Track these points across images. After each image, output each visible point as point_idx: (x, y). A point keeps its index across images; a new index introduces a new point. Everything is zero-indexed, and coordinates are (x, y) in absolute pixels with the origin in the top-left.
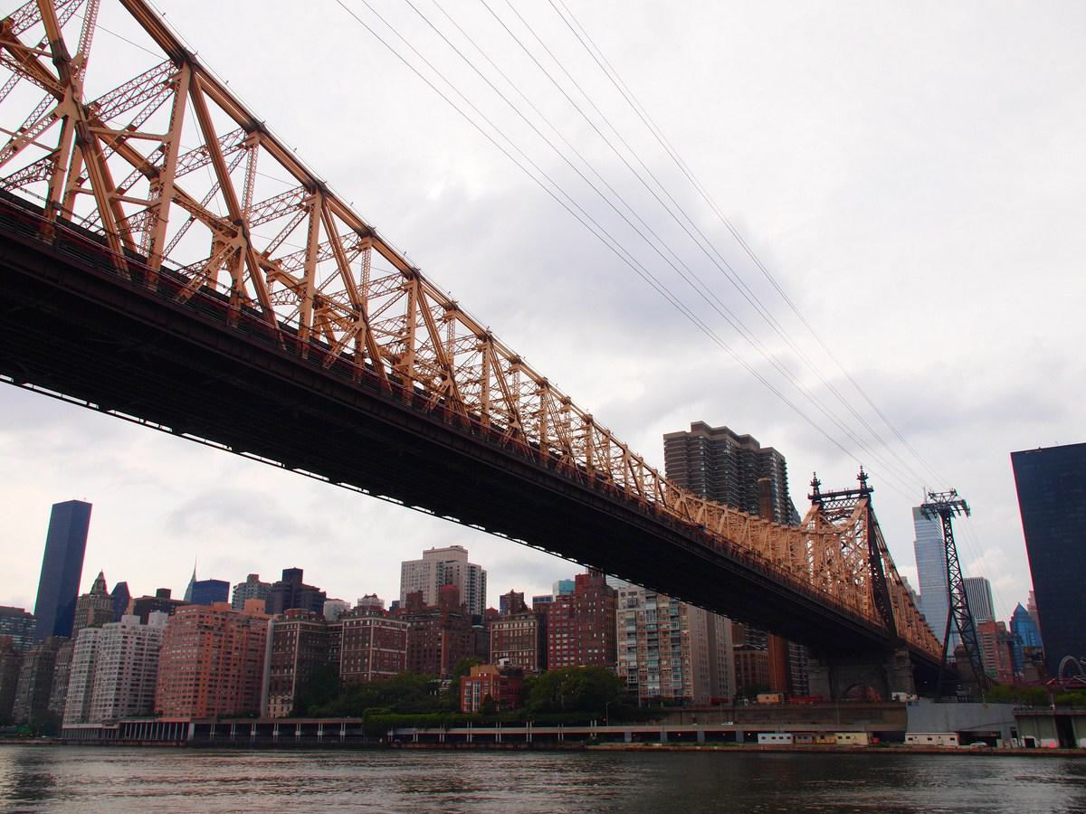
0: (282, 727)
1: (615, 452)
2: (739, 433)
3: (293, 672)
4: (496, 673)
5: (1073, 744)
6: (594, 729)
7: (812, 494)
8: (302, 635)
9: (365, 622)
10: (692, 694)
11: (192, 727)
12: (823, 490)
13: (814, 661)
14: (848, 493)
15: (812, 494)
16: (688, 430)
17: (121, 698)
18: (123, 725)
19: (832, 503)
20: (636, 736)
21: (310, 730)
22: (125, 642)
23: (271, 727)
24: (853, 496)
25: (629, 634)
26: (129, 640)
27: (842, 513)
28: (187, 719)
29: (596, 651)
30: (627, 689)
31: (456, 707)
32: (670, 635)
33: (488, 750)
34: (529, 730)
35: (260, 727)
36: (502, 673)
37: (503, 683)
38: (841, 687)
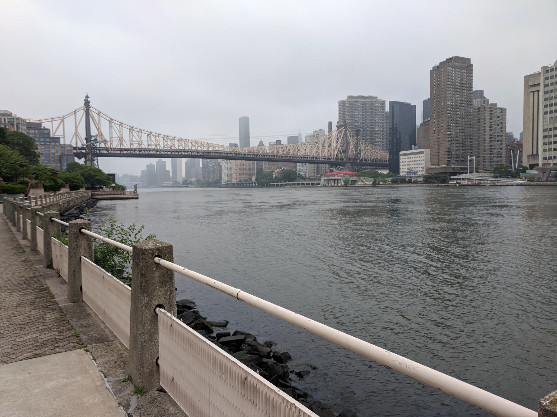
3: (255, 171)
4: (279, 171)
34: (279, 183)
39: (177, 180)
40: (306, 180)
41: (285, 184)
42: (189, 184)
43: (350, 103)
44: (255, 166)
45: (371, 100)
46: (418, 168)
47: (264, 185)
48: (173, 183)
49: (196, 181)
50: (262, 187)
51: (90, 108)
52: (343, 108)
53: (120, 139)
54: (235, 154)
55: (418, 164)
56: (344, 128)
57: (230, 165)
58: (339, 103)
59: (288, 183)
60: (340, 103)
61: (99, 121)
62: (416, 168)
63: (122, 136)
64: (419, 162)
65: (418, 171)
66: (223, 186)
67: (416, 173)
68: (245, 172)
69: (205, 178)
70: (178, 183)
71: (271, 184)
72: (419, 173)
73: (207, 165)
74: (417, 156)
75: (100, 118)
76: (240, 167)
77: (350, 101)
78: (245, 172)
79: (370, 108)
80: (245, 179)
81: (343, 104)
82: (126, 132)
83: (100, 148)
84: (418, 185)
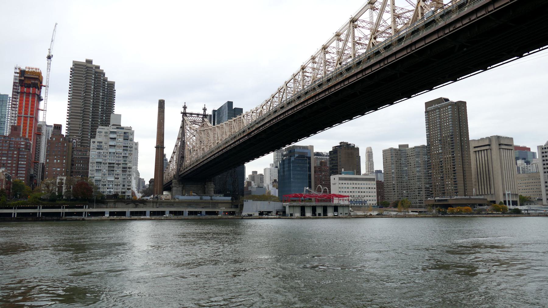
5: (304, 215)
6: (86, 210)
7: (183, 112)
12: (188, 111)
14: (198, 115)
15: (183, 112)
19: (197, 118)
20: (208, 213)
22: (454, 163)
24: (200, 116)
27: (194, 122)
29: (59, 169)
32: (121, 166)
46: (367, 196)
55: (367, 192)
62: (364, 196)
64: (368, 190)
65: (367, 200)
67: (365, 202)
72: (368, 202)
74: (365, 182)
84: (505, 215)
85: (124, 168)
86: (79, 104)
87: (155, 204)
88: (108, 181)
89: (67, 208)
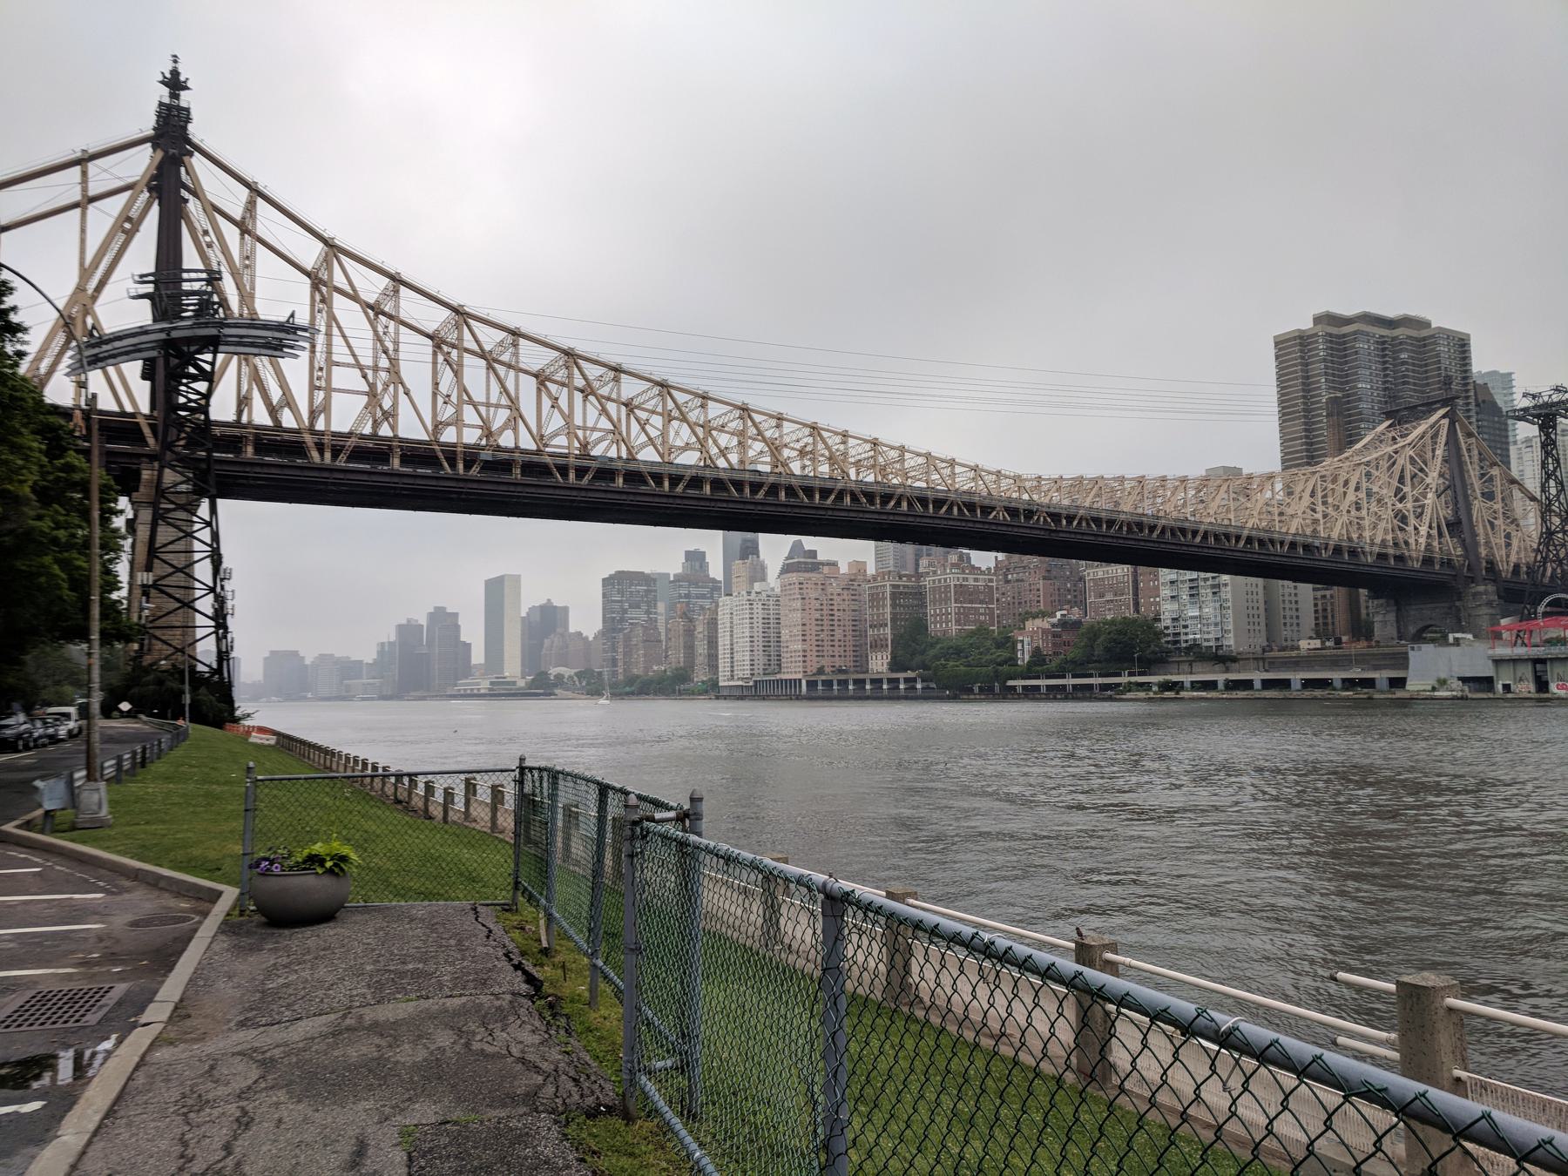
0: (873, 681)
1: (911, 461)
2: (1391, 312)
3: (888, 630)
4: (1047, 626)
8: (893, 594)
9: (945, 580)
10: (1232, 642)
11: (804, 683)
13: (1381, 601)
16: (1307, 324)
17: (756, 658)
18: (756, 682)
21: (894, 682)
23: (863, 681)
25: (1172, 582)
26: (755, 606)
28: (799, 676)
30: (1169, 639)
31: (1012, 661)
33: (1035, 699)
34: (1070, 681)
35: (856, 682)
36: (1053, 625)
37: (1055, 635)
38: (1412, 629)
39: (502, 672)
40: (1235, 666)
41: (1105, 687)
42: (555, 686)
43: (1331, 342)
44: (888, 610)
45: (1414, 333)
47: (971, 691)
48: (492, 683)
49: (576, 674)
50: (954, 698)
51: (191, 154)
52: (1302, 364)
53: (372, 394)
54: (1007, 509)
56: (1444, 417)
57: (760, 611)
58: (1277, 344)
59: (1133, 679)
60: (1281, 343)
61: (248, 257)
63: (394, 362)
66: (725, 693)
68: (838, 634)
69: (615, 666)
70: (508, 683)
71: (1010, 683)
73: (622, 620)
75: (253, 250)
76: (818, 616)
77: (1331, 335)
78: (838, 634)
79: (1414, 365)
80: (838, 662)
81: (1301, 344)
82: (415, 357)
83: (244, 427)
85: (1213, 586)
86: (1296, 432)
87: (1261, 664)
88: (1192, 618)
89: (1101, 676)
